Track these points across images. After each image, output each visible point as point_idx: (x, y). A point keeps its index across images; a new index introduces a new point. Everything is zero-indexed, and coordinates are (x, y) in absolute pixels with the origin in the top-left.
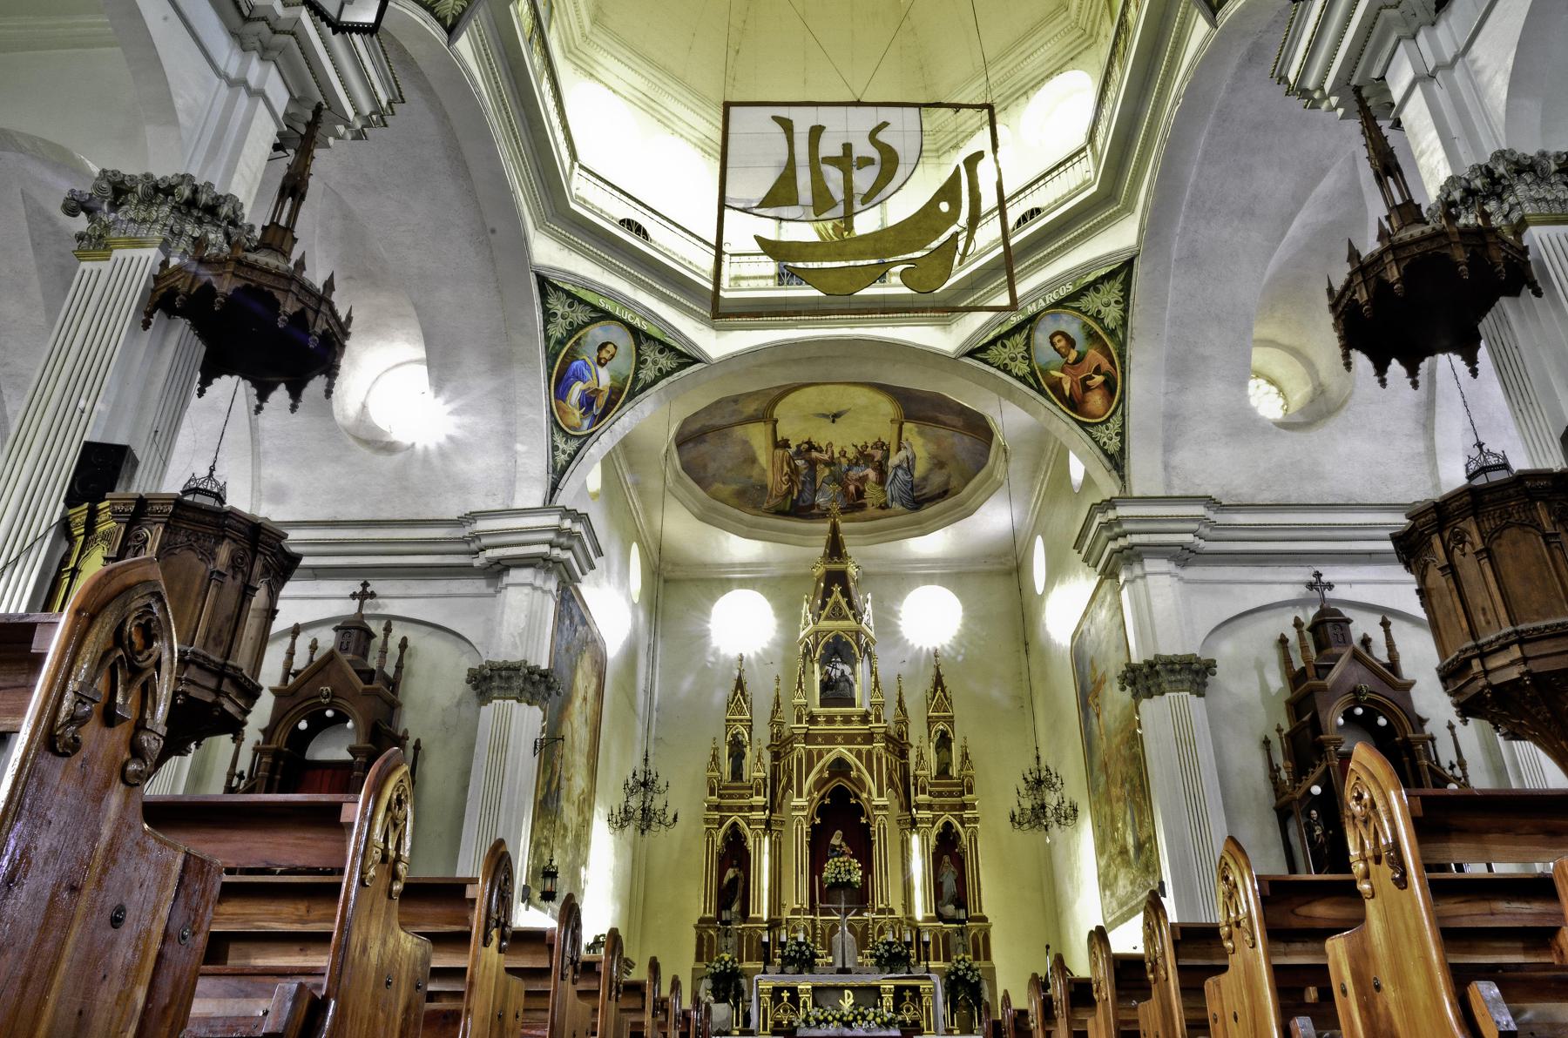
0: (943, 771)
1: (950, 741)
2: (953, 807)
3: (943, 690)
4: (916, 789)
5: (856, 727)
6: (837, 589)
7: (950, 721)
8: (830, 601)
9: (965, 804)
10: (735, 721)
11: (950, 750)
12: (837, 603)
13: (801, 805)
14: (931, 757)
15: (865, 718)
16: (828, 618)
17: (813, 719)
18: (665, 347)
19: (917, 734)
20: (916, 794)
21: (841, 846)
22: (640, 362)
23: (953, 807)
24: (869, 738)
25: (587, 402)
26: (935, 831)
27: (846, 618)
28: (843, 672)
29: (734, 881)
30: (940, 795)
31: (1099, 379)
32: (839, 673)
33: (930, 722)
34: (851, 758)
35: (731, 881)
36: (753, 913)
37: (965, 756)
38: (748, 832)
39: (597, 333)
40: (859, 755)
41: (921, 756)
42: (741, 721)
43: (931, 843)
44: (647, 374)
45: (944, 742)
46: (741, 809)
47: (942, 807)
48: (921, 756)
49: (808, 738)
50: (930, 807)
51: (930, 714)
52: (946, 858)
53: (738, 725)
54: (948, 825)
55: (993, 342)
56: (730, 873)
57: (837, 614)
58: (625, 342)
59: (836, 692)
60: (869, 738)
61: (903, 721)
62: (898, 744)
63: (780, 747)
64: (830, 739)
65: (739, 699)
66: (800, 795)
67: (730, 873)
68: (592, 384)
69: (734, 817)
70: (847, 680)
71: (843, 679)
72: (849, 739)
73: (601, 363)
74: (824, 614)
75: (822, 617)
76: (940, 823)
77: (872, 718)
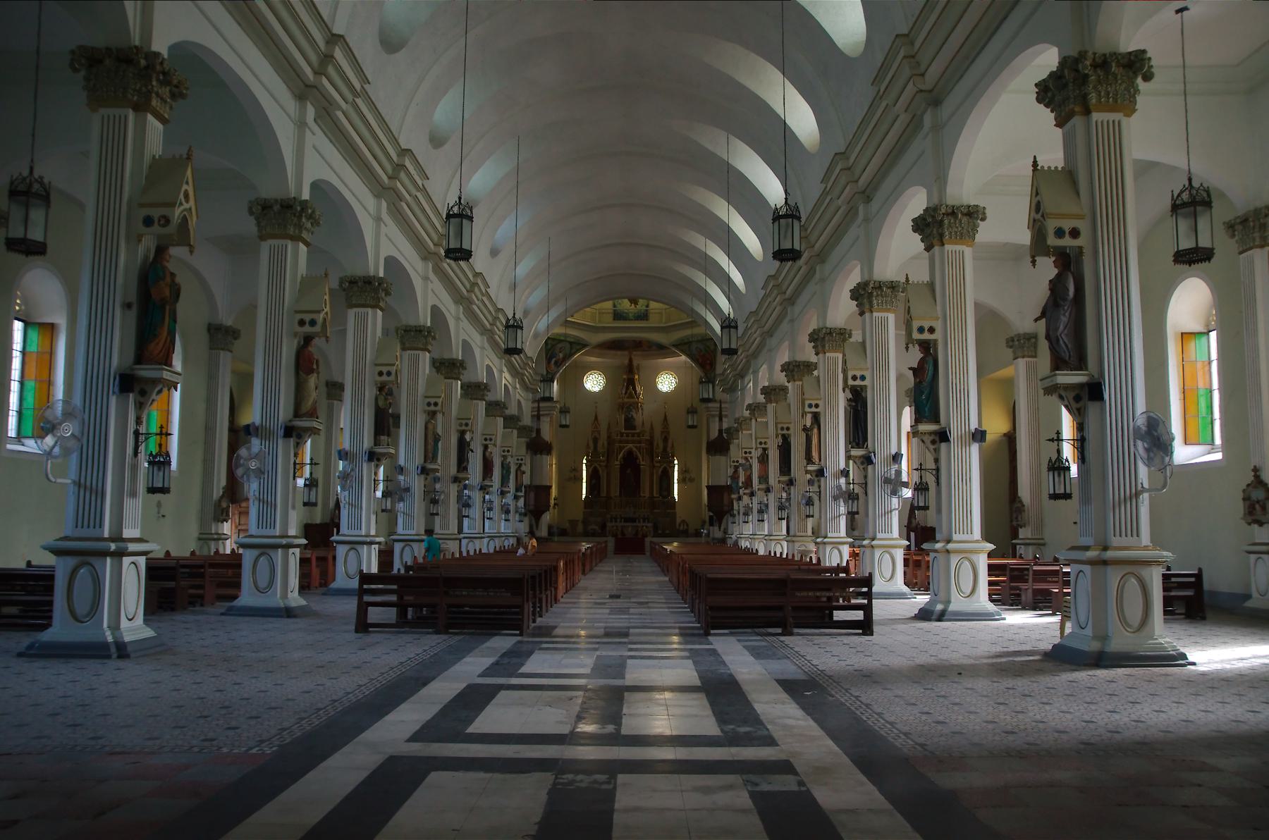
5: (636, 438)
13: (617, 463)
14: (661, 445)
15: (638, 435)
17: (622, 434)
18: (579, 344)
22: (571, 349)
24: (640, 442)
25: (556, 363)
31: (708, 362)
34: (634, 449)
39: (560, 345)
40: (636, 447)
44: (573, 351)
45: (666, 440)
49: (620, 442)
55: (679, 345)
58: (568, 346)
59: (629, 423)
60: (640, 442)
61: (652, 437)
63: (610, 441)
64: (628, 442)
66: (617, 461)
68: (558, 357)
72: (633, 442)
73: (560, 352)
77: (641, 435)
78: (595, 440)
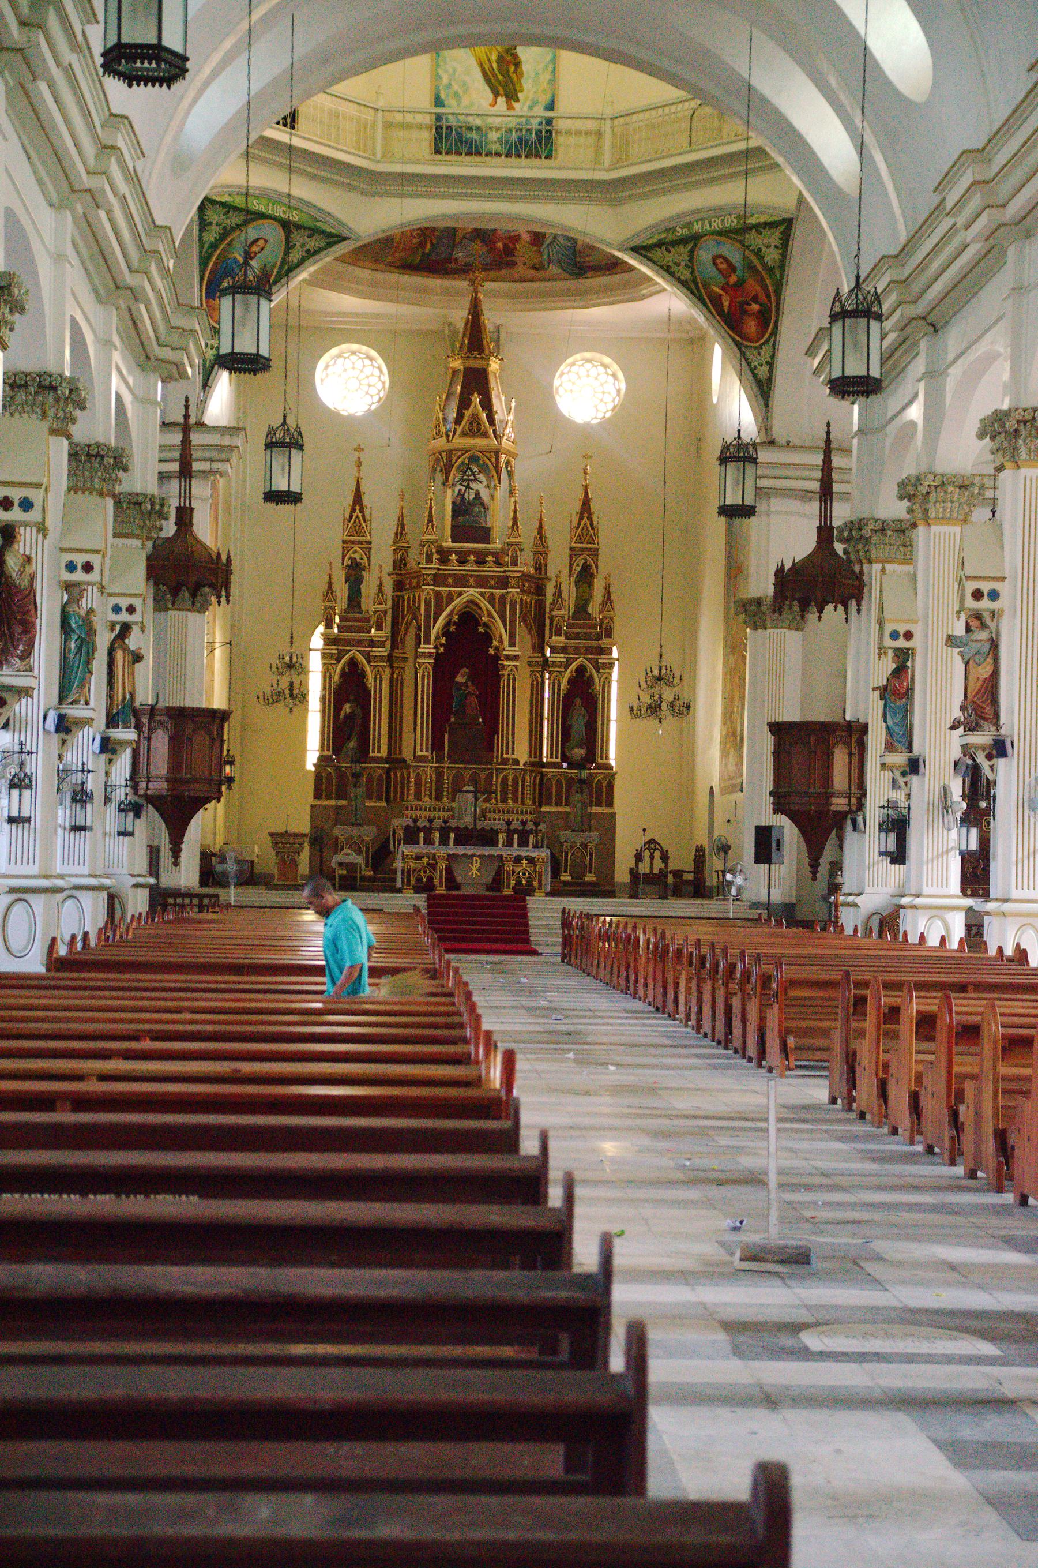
0: (581, 609)
1: (592, 575)
2: (589, 650)
3: (590, 518)
4: (551, 629)
6: (476, 399)
7: (595, 553)
8: (467, 414)
9: (601, 648)
10: (353, 542)
11: (590, 584)
12: (475, 417)
14: (570, 593)
16: (464, 434)
19: (558, 564)
20: (550, 638)
21: (466, 685)
23: (589, 650)
26: (567, 675)
27: (485, 435)
28: (478, 494)
29: (349, 717)
30: (577, 637)
32: (472, 496)
33: (573, 553)
35: (346, 716)
36: (373, 752)
37: (608, 595)
38: (367, 668)
41: (558, 593)
42: (360, 542)
43: (562, 687)
45: (585, 576)
46: (359, 643)
47: (577, 650)
48: (558, 593)
50: (564, 650)
51: (573, 545)
52: (578, 701)
53: (356, 547)
54: (581, 670)
56: (347, 708)
57: (475, 430)
62: (536, 584)
65: (357, 517)
67: (347, 708)
69: (354, 652)
70: (483, 505)
71: (477, 502)
74: (459, 429)
75: (458, 433)
76: (574, 666)
78: (355, 573)
